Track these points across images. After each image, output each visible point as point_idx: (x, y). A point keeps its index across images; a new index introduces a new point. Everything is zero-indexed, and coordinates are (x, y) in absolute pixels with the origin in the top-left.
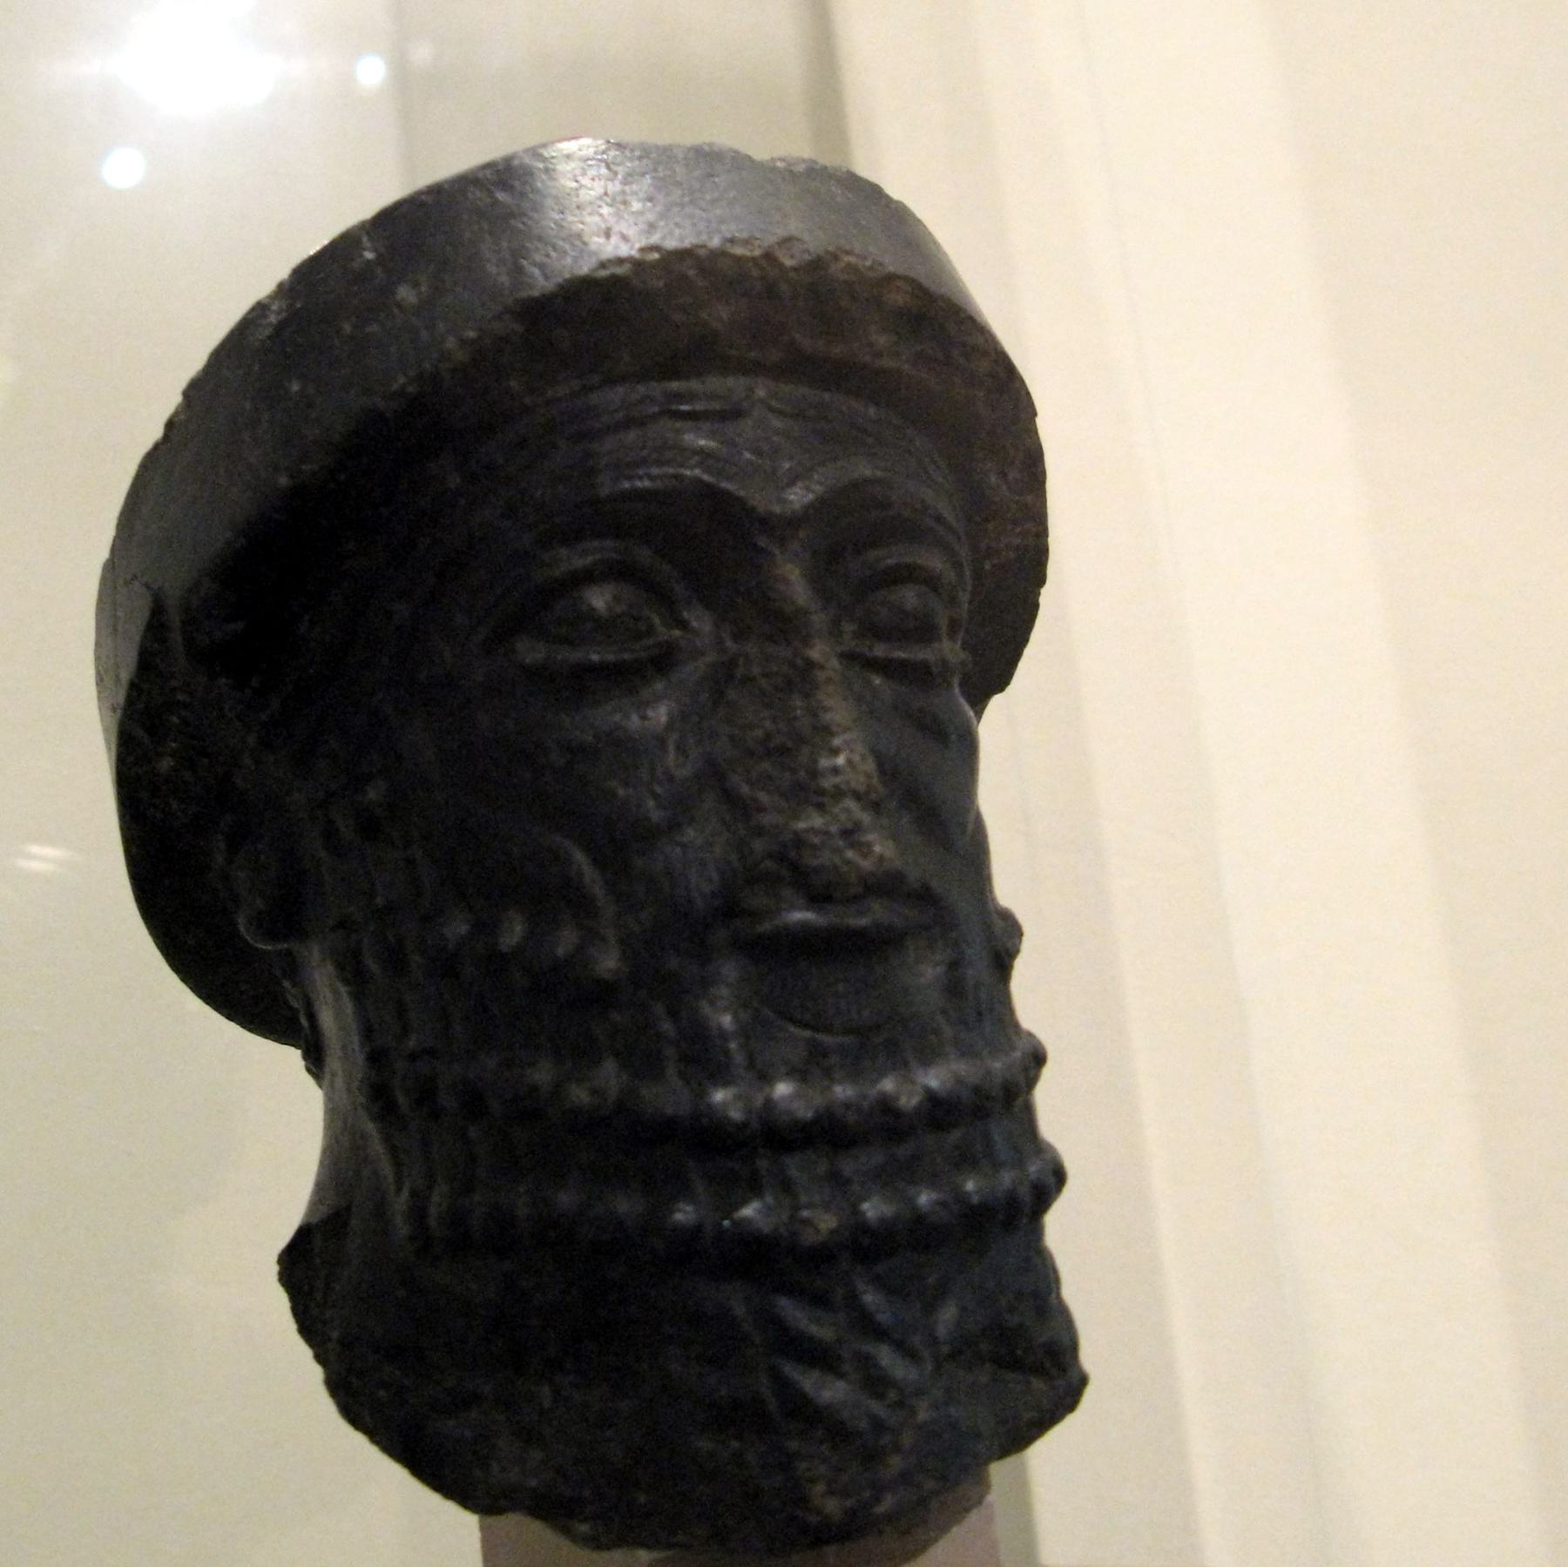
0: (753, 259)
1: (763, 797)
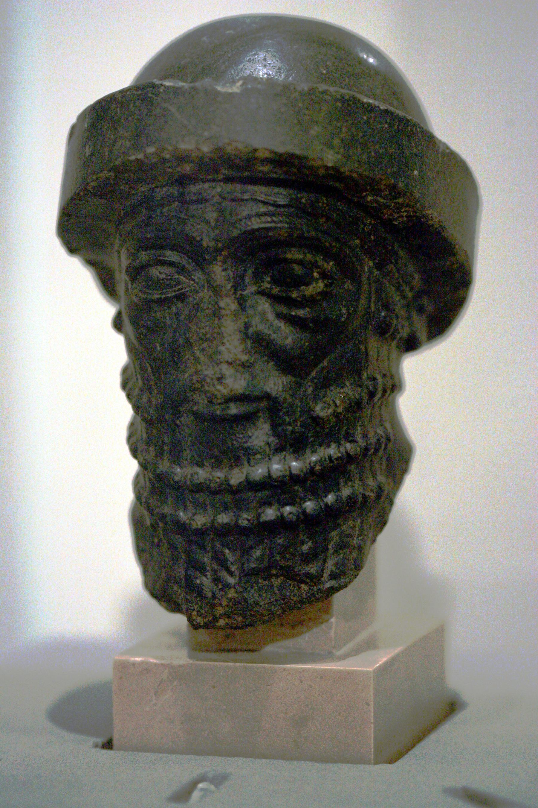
1: (202, 358)
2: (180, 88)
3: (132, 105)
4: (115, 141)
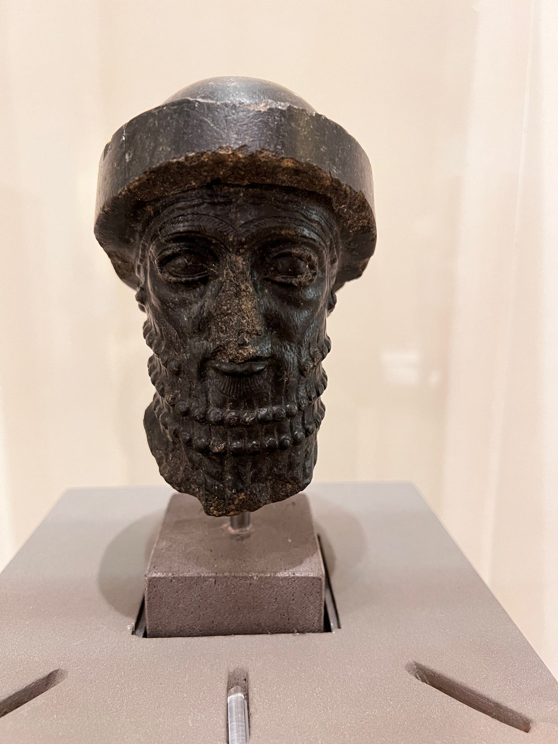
0: (229, 155)
2: (212, 104)
3: (169, 118)
4: (155, 148)
